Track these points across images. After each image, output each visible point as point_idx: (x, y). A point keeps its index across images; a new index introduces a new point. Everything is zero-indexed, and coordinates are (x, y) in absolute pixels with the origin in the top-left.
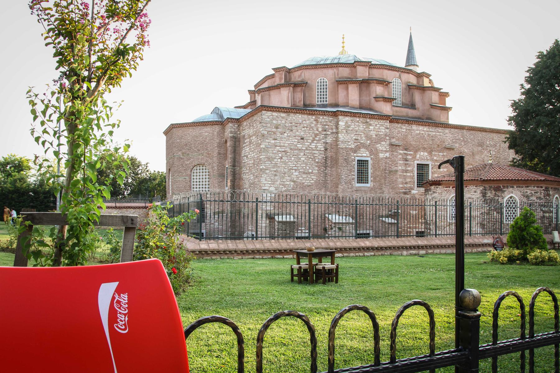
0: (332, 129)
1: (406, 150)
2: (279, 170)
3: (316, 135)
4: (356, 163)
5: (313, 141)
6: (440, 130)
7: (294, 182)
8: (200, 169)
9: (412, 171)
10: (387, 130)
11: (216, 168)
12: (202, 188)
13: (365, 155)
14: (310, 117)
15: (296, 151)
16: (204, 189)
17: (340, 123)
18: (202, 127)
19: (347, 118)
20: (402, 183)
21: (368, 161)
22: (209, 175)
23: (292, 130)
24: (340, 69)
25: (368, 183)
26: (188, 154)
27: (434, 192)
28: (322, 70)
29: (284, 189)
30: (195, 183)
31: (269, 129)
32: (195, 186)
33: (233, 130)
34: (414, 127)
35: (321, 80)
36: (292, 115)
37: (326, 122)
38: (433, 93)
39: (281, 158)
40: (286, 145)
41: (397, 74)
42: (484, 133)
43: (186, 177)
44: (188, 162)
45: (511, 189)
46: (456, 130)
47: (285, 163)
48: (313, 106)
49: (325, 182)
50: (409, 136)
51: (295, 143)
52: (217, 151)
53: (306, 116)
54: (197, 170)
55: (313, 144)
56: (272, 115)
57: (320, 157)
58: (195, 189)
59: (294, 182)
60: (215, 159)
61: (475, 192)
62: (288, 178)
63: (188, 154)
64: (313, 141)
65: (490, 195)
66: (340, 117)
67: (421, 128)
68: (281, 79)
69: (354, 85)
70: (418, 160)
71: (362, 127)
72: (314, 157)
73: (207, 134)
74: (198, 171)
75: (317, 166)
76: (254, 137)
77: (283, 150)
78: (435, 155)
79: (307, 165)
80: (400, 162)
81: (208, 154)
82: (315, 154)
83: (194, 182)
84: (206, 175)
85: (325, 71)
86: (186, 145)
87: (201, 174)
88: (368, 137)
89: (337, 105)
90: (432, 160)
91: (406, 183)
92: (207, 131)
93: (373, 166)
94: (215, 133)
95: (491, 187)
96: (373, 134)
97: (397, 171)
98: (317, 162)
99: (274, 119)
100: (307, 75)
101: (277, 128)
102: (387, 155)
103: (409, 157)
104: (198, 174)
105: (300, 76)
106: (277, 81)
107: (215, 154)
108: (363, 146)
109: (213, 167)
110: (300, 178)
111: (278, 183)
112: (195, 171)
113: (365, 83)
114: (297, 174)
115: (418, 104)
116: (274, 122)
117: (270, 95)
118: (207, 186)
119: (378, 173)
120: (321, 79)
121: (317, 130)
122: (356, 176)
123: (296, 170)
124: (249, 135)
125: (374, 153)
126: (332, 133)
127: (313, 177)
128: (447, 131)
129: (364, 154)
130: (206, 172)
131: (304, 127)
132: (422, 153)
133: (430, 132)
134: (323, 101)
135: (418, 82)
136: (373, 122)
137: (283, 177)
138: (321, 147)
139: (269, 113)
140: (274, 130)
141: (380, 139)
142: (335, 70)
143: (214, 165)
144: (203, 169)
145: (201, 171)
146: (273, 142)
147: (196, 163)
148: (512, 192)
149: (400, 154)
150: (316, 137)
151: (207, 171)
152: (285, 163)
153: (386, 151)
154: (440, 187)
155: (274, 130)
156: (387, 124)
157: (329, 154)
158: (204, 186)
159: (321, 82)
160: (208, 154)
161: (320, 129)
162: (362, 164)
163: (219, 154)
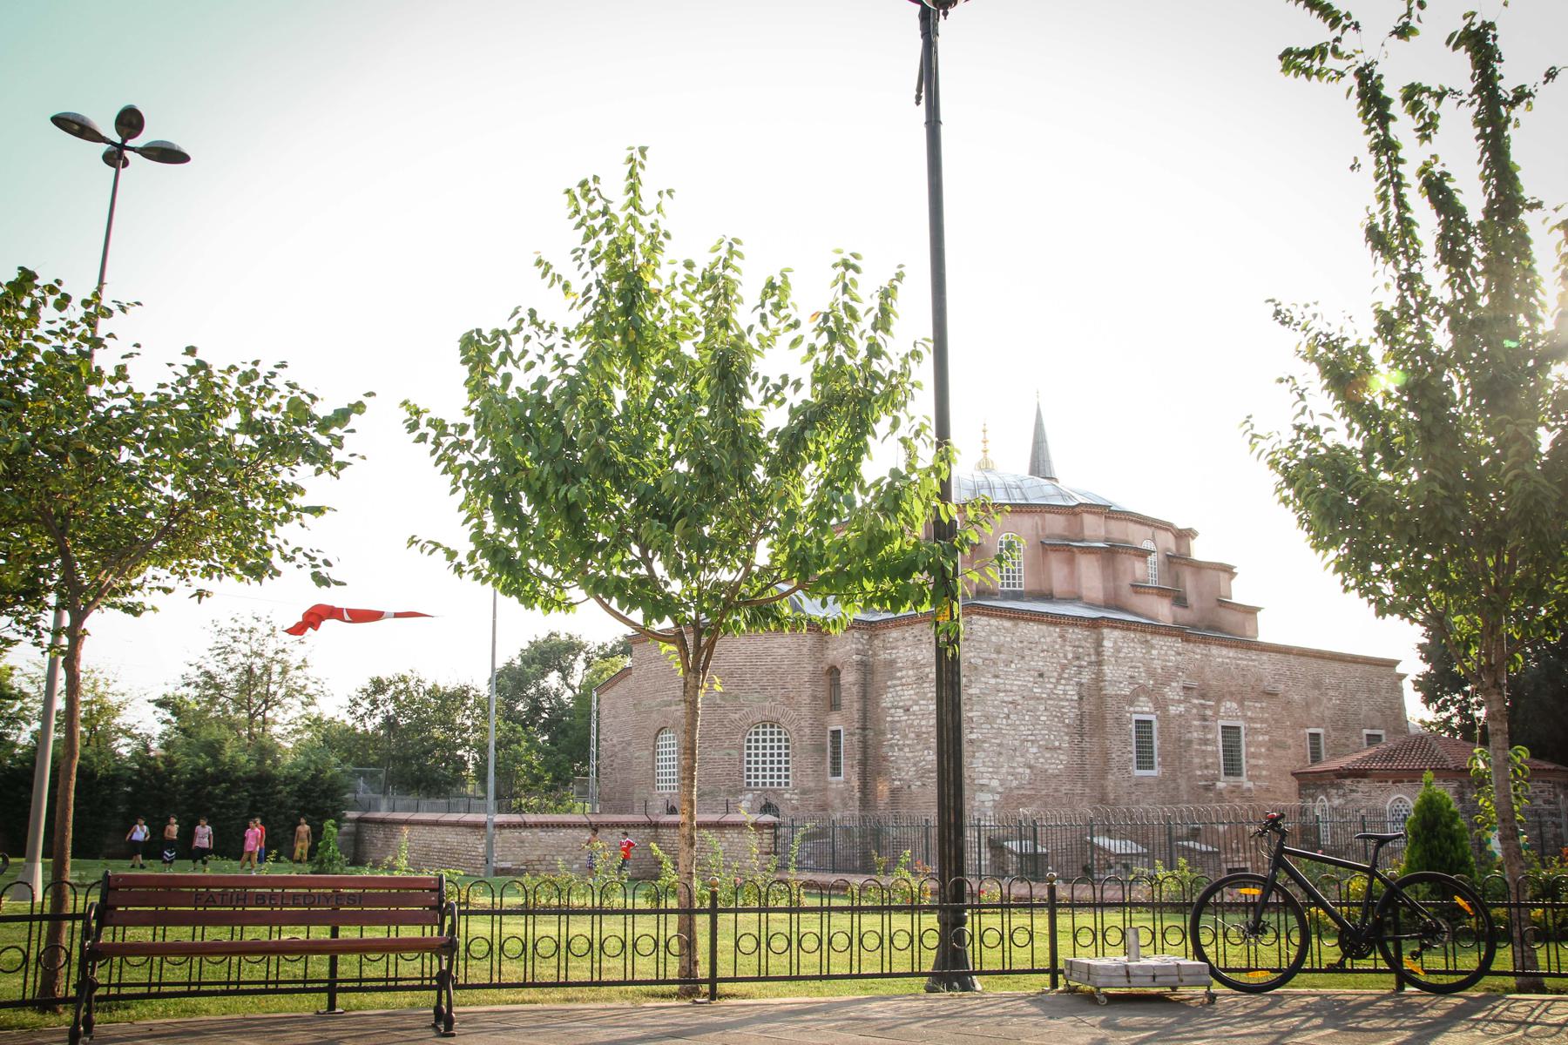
1: (1203, 696)
3: (1064, 667)
4: (1133, 726)
6: (1253, 655)
7: (1030, 767)
8: (764, 733)
9: (1215, 742)
11: (807, 731)
16: (776, 780)
17: (1106, 643)
19: (1117, 633)
20: (1201, 768)
22: (787, 748)
24: (1048, 516)
25: (1152, 768)
26: (737, 697)
27: (1352, 791)
29: (1015, 784)
31: (985, 655)
34: (1215, 650)
36: (1022, 624)
38: (1222, 574)
41: (1149, 531)
42: (1320, 662)
46: (1279, 656)
47: (1015, 727)
48: (991, 594)
49: (1082, 766)
50: (1207, 669)
53: (1044, 627)
58: (753, 780)
60: (804, 710)
63: (737, 697)
66: (1106, 631)
67: (1225, 651)
69: (1092, 557)
71: (1140, 651)
73: (783, 651)
74: (761, 737)
78: (1249, 708)
79: (1050, 731)
80: (1196, 723)
84: (779, 748)
88: (1151, 673)
89: (1047, 597)
90: (1245, 717)
91: (1207, 767)
93: (1161, 733)
94: (805, 650)
96: (1157, 664)
97: (1190, 742)
98: (1068, 726)
99: (993, 633)
102: (1182, 708)
103: (1209, 712)
104: (761, 744)
107: (805, 698)
108: (1141, 690)
109: (799, 729)
111: (1004, 770)
113: (1112, 552)
114: (1034, 750)
115: (1192, 598)
116: (994, 639)
119: (1170, 747)
122: (1134, 756)
124: (915, 662)
125: (1161, 705)
126: (1090, 663)
128: (1265, 657)
129: (1145, 709)
132: (1228, 704)
135: (1178, 549)
136: (1156, 640)
137: (1013, 758)
138: (1072, 693)
139: (984, 620)
140: (994, 656)
141: (1168, 678)
146: (993, 681)
147: (758, 717)
149: (1195, 706)
152: (1015, 727)
153: (1180, 702)
155: (994, 656)
156: (1179, 645)
157: (1086, 708)
158: (776, 773)
161: (1070, 656)
162: (1144, 726)
163: (815, 698)
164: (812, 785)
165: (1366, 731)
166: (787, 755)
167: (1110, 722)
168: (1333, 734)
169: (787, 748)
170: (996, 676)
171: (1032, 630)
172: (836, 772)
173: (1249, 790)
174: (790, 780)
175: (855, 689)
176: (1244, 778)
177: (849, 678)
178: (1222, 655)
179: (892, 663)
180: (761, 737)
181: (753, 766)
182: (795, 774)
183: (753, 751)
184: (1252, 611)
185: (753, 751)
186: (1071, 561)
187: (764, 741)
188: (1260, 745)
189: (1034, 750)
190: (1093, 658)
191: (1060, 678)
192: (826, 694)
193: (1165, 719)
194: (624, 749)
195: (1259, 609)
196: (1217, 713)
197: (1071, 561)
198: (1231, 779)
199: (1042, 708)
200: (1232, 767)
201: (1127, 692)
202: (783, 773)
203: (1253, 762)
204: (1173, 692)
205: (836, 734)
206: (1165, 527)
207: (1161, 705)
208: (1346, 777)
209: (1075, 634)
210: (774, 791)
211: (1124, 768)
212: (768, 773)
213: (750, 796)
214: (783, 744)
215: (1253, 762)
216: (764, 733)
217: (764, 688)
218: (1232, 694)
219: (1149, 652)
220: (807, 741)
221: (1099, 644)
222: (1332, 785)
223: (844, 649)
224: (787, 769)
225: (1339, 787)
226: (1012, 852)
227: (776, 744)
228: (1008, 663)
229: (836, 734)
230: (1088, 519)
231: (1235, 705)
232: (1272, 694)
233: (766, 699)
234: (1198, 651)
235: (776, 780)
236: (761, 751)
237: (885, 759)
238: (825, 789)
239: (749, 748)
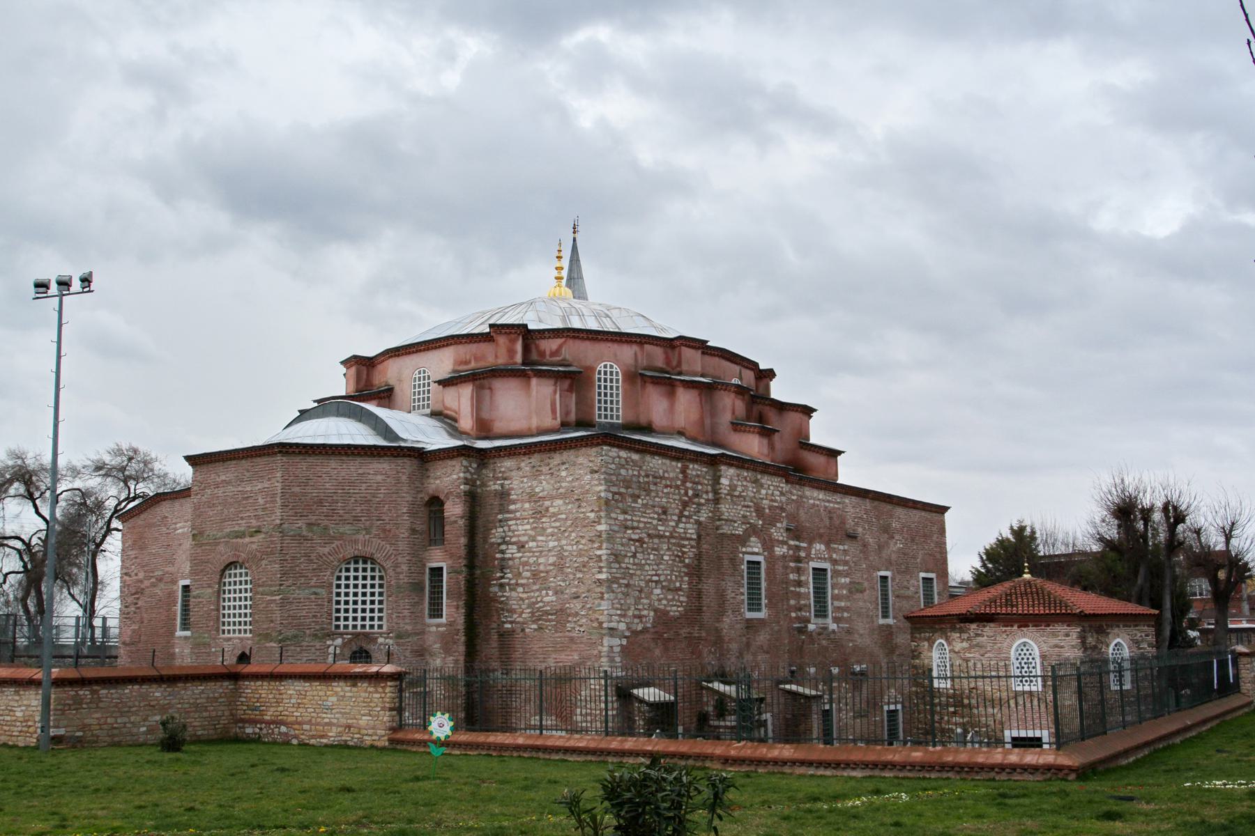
0: (707, 492)
2: (632, 582)
3: (685, 505)
4: (744, 567)
5: (679, 521)
8: (356, 570)
9: (807, 583)
10: (784, 499)
11: (405, 568)
12: (363, 619)
13: (756, 550)
14: (674, 463)
15: (656, 541)
16: (368, 623)
18: (368, 460)
19: (732, 471)
21: (759, 563)
22: (381, 586)
23: (648, 492)
25: (759, 610)
26: (326, 528)
27: (977, 635)
28: (609, 344)
29: (640, 628)
30: (342, 607)
32: (342, 615)
33: (468, 476)
34: (808, 492)
35: (609, 368)
36: (648, 458)
37: (698, 476)
39: (634, 556)
40: (642, 525)
41: (737, 368)
43: (319, 590)
44: (326, 550)
45: (1116, 630)
47: (641, 566)
51: (655, 522)
52: (407, 524)
53: (668, 462)
54: (348, 570)
55: (681, 525)
56: (619, 457)
57: (691, 555)
58: (342, 623)
59: (656, 611)
60: (402, 546)
61: (1067, 635)
62: (645, 601)
63: (326, 528)
64: (679, 521)
65: (1091, 640)
66: (723, 468)
67: (815, 493)
68: (511, 352)
70: (812, 559)
72: (684, 553)
73: (379, 478)
74: (352, 574)
75: (686, 574)
76: (560, 502)
77: (636, 537)
78: (835, 550)
80: (792, 564)
81: (384, 531)
82: (684, 546)
83: (338, 603)
85: (615, 347)
86: (320, 503)
87: (360, 582)
88: (759, 511)
92: (379, 469)
93: (767, 574)
94: (404, 478)
95: (1091, 626)
98: (687, 566)
99: (623, 466)
100: (575, 352)
101: (627, 488)
103: (803, 554)
104: (352, 582)
105: (555, 353)
106: (493, 356)
107: (404, 533)
108: (753, 530)
109: (396, 566)
110: (664, 602)
112: (344, 574)
116: (623, 472)
117: (490, 388)
118: (376, 615)
120: (605, 366)
121: (686, 494)
122: (745, 597)
123: (656, 582)
127: (682, 599)
129: (754, 550)
130: (373, 578)
131: (666, 486)
133: (829, 501)
134: (612, 417)
137: (638, 600)
138: (692, 531)
140: (623, 490)
142: (635, 348)
143: (400, 559)
144: (365, 570)
145: (360, 574)
146: (621, 517)
148: (1118, 636)
150: (684, 509)
151: (377, 574)
154: (992, 625)
158: (368, 615)
159: (605, 373)
160: (384, 531)
161: (690, 493)
163: (413, 531)
164: (409, 628)
165: (923, 575)
166: (381, 594)
167: (726, 562)
168: (898, 577)
169: (381, 586)
170: (625, 512)
171: (656, 463)
172: (436, 612)
173: (834, 631)
174: (384, 622)
175: (461, 522)
176: (829, 620)
177: (454, 510)
178: (815, 497)
179: (504, 495)
180: (352, 574)
181: (342, 607)
182: (390, 616)
183: (343, 590)
184: (834, 454)
185: (343, 590)
186: (671, 394)
187: (356, 578)
188: (842, 587)
189: (658, 591)
190: (711, 496)
191: (681, 516)
192: (424, 527)
193: (771, 560)
194: (153, 585)
195: (840, 453)
196: (808, 555)
197: (671, 394)
198: (820, 621)
199: (665, 547)
200: (821, 612)
201: (740, 532)
202: (376, 615)
203: (837, 603)
204: (778, 532)
205: (437, 572)
206: (752, 365)
207: (768, 545)
208: (972, 621)
209: (695, 469)
210: (366, 635)
211: (736, 611)
212: (359, 615)
213: (339, 641)
214: (377, 582)
215: (837, 603)
216: (356, 570)
217: (357, 519)
218: (821, 536)
219: (759, 492)
220: (404, 579)
221: (716, 480)
222: (953, 629)
223: (449, 479)
224: (380, 610)
225: (961, 631)
226: (642, 701)
227: (369, 582)
228: (635, 497)
229: (437, 572)
230: (688, 353)
231: (823, 547)
232: (852, 537)
233: (358, 532)
234: (796, 492)
235: (368, 623)
236: (351, 590)
237: (495, 599)
238: (423, 633)
239: (339, 586)
